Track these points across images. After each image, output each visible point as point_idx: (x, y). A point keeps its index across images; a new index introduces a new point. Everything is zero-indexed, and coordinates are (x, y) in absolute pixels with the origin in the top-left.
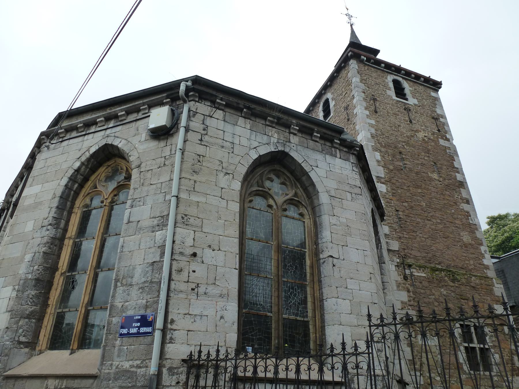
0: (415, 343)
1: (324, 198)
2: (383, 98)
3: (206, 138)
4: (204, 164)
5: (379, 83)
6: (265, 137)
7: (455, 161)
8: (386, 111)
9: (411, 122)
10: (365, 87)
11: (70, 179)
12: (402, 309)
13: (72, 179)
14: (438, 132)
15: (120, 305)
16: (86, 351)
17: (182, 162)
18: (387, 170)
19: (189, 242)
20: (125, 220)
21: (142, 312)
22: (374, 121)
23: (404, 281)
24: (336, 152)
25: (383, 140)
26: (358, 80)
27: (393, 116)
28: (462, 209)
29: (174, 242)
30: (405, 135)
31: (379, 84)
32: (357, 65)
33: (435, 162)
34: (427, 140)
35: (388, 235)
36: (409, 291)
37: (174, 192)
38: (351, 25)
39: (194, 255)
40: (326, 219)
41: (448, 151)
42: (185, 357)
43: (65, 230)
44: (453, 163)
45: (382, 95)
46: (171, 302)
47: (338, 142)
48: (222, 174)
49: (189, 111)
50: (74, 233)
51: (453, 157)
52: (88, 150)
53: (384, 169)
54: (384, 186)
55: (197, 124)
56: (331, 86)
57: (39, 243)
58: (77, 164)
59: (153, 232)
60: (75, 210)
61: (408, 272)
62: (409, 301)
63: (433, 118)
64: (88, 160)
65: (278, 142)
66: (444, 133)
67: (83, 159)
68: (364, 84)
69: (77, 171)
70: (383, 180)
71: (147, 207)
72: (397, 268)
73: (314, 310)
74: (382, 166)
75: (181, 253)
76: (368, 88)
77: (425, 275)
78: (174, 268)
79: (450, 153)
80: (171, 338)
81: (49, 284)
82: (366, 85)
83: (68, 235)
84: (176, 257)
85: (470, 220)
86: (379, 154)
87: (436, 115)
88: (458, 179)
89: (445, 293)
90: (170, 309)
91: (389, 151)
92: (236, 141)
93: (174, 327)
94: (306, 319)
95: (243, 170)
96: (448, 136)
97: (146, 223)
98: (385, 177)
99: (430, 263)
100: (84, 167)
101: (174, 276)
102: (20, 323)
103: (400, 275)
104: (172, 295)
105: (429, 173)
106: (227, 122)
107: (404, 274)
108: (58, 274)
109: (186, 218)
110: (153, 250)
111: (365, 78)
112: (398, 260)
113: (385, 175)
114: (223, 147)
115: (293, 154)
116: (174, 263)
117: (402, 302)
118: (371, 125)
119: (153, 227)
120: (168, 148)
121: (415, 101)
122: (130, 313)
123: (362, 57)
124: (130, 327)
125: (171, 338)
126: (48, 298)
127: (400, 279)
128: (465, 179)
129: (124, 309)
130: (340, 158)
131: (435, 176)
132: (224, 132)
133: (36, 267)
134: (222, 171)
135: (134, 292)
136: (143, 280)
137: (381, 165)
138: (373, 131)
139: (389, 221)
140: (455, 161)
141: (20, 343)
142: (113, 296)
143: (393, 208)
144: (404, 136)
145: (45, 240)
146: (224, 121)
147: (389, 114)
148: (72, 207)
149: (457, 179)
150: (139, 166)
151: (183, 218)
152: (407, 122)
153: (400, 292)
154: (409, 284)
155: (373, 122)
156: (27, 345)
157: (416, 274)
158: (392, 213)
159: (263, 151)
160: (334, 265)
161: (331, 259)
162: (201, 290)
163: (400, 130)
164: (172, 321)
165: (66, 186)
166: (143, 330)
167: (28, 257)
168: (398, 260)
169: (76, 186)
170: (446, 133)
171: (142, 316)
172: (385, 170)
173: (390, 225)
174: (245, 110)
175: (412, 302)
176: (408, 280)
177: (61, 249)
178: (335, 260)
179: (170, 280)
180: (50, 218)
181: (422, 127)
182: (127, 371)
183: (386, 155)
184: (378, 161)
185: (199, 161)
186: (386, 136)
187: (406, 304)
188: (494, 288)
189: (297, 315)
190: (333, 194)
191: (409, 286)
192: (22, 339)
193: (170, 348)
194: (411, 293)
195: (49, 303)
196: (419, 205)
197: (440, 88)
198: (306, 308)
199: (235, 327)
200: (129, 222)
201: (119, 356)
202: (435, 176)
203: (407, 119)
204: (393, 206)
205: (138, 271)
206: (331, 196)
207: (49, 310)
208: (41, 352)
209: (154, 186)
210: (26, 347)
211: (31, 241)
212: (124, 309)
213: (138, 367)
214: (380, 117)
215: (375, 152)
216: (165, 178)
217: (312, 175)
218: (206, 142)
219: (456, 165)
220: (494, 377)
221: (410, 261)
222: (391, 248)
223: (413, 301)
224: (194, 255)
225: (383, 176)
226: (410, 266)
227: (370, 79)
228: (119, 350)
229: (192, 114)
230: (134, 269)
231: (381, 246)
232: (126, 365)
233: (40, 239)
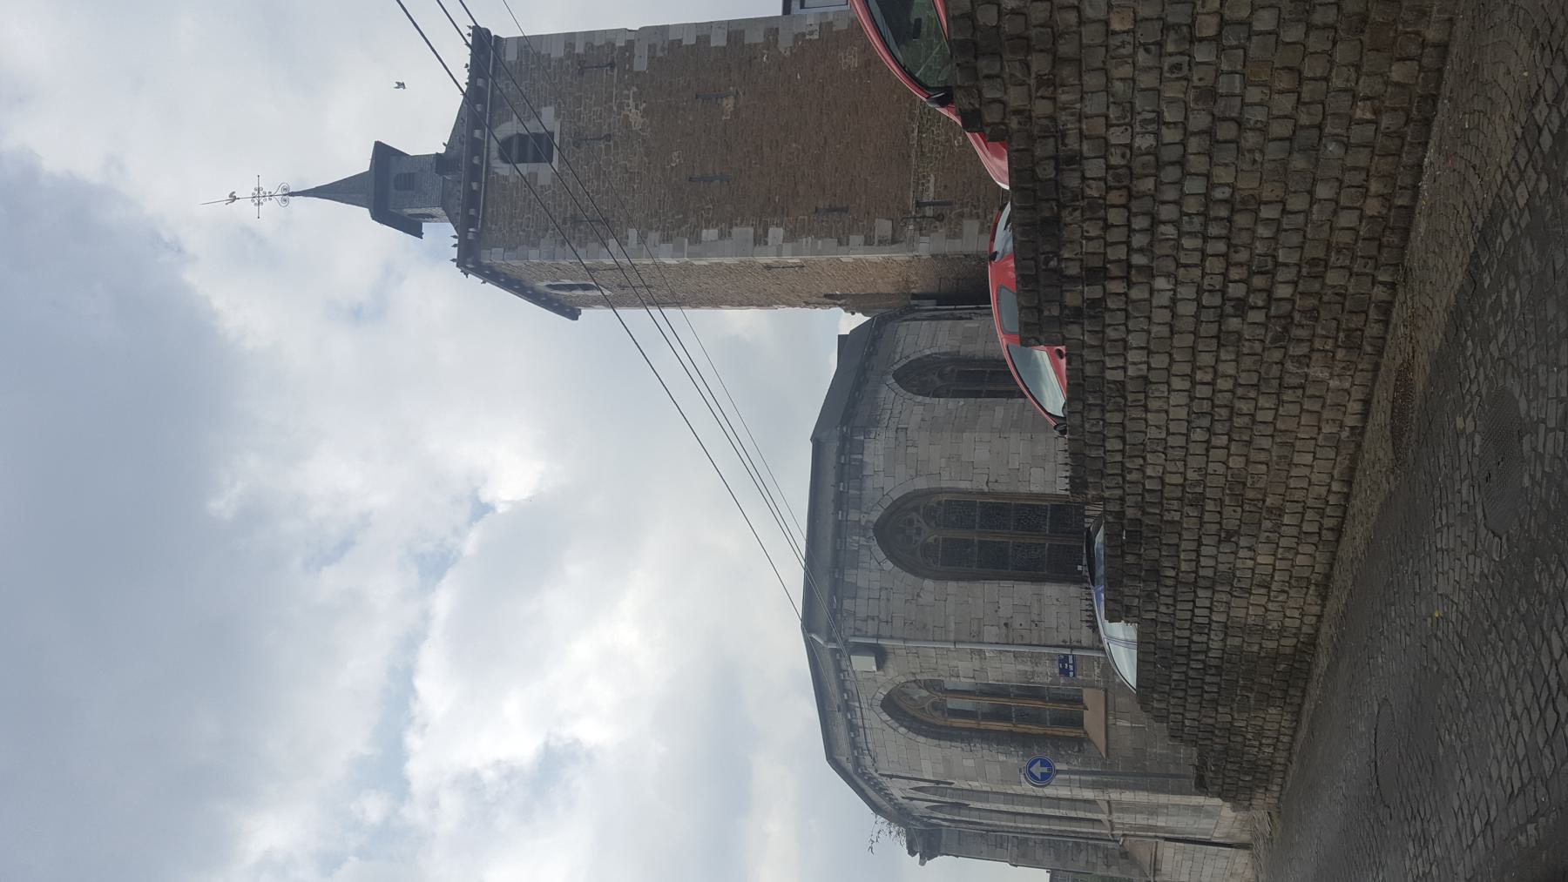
1: (922, 484)
2: (563, 198)
3: (882, 616)
4: (914, 618)
5: (525, 199)
6: (863, 551)
7: (681, 41)
8: (596, 197)
9: (608, 137)
10: (548, 236)
11: (918, 734)
13: (918, 732)
14: (616, 70)
15: (1051, 678)
16: (1085, 698)
17: (915, 640)
18: (737, 219)
19: (995, 630)
20: (973, 681)
21: (1056, 662)
22: (630, 230)
23: (945, 221)
24: (855, 460)
25: (670, 214)
26: (533, 253)
27: (604, 182)
28: (791, 51)
29: (997, 643)
30: (646, 159)
31: (527, 201)
32: (493, 249)
33: (694, 96)
34: (644, 105)
35: (865, 236)
36: (961, 215)
37: (952, 647)
38: (292, 194)
39: (1006, 625)
40: (945, 485)
41: (659, 54)
42: (1091, 631)
43: (970, 729)
44: (687, 46)
45: (558, 198)
46: (1049, 643)
47: (843, 457)
48: (920, 599)
49: (854, 636)
50: (973, 722)
51: (672, 42)
52: (885, 722)
53: (736, 225)
54: (772, 231)
55: (871, 627)
56: (519, 282)
57: (988, 751)
58: (902, 730)
59: (985, 659)
60: (948, 723)
61: (929, 211)
63: (581, 73)
64: (897, 720)
65: (864, 536)
66: (616, 53)
67: (897, 725)
68: (542, 240)
69: (909, 729)
70: (760, 231)
71: (960, 664)
72: (924, 232)
73: (1041, 500)
74: (731, 228)
75: (1007, 636)
76: (547, 230)
77: (932, 178)
78: (1020, 642)
79: (663, 49)
80: (1078, 642)
81: (1025, 735)
82: (540, 234)
83: (975, 726)
84: (1010, 642)
85: (811, 37)
86: (704, 231)
87: (569, 62)
88: (723, 43)
89: (960, 138)
90: (1055, 644)
91: (691, 206)
92: (877, 585)
93: (1068, 639)
94: (1049, 509)
95: (910, 578)
96: (620, 43)
97: (977, 664)
98: (752, 225)
99: (909, 156)
100: (905, 723)
101: (1028, 642)
102: (1063, 753)
103: (936, 227)
104: (1043, 643)
105: (724, 118)
106: (856, 594)
107: (934, 220)
108: (1014, 729)
109: (973, 634)
110: (1003, 658)
111: (521, 233)
112: (911, 227)
113: (748, 225)
114: (888, 600)
115: (875, 520)
116: (1015, 642)
118: (642, 238)
119: (981, 658)
120: (897, 651)
121: (548, 113)
122: (1057, 671)
123: (470, 237)
124: (1068, 670)
125: (1078, 642)
126: (1039, 734)
127: (943, 231)
128: (720, 24)
129: (1053, 675)
130: (862, 454)
131: (729, 104)
132: (869, 599)
133: (1013, 749)
134: (917, 600)
135: (1039, 669)
136: (1029, 663)
137: (727, 230)
138: (654, 236)
139: (841, 231)
140: (681, 41)
141: (1079, 751)
142: (1042, 684)
143: (812, 218)
144: (649, 163)
145: (985, 746)
146: (855, 598)
147: (602, 189)
148: (945, 727)
149: (725, 48)
150: (914, 674)
151: (974, 636)
152: (610, 146)
154: (950, 213)
155: (633, 233)
156: (1081, 745)
157: (932, 195)
158: (823, 221)
159: (881, 555)
160: (996, 481)
161: (989, 484)
162: (1036, 618)
163: (636, 170)
164: (1064, 641)
165: (926, 736)
166: (1071, 662)
167: (1002, 758)
168: (911, 227)
169: (924, 727)
170: (614, 45)
171: (1060, 663)
172: (739, 221)
173: (847, 231)
174: (837, 576)
175: (980, 211)
176: (944, 212)
177: (991, 731)
178: (990, 480)
179: (1031, 645)
180: (963, 745)
181: (615, 109)
182: (1102, 671)
183: (705, 216)
184: (722, 236)
185: (911, 623)
186: (660, 205)
187: (982, 224)
189: (1045, 517)
190: (913, 472)
191: (953, 213)
192: (1076, 749)
193: (1084, 644)
194: (965, 209)
195: (1042, 732)
196: (798, 158)
197: (488, 32)
198: (1038, 506)
199: (1064, 587)
200: (973, 678)
201: (1091, 676)
202: (729, 104)
203: (603, 147)
204: (809, 218)
205: (1021, 667)
206: (917, 474)
207: (1049, 732)
208: (1086, 733)
209: (939, 660)
210: (1082, 745)
211: (986, 758)
212: (1053, 675)
213: (1099, 663)
214: (616, 214)
215: (703, 239)
216: (933, 653)
217: (896, 495)
218: (887, 616)
219: (690, 40)
221: (911, 202)
222: (890, 237)
224: (1006, 625)
225: (751, 230)
226: (919, 204)
227: (520, 221)
228: (1087, 676)
229: (857, 632)
230: (1019, 671)
231: (936, 354)
232: (1097, 671)
233: (984, 751)
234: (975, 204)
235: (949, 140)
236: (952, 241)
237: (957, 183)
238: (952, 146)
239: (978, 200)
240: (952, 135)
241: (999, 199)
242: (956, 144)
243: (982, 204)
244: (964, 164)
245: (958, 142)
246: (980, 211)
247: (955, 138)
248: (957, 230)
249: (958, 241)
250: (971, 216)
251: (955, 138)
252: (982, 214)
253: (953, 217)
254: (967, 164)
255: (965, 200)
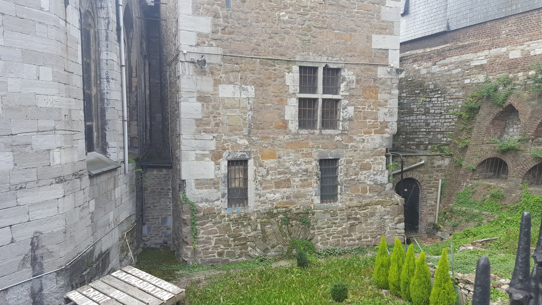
0: (211, 96)
12: (198, 45)
36: (216, 16)
62: (213, 32)
89: (287, 18)
117: (199, 35)
153: (198, 18)
154: (218, 5)
175: (220, 34)
187: (207, 36)
188: (383, 7)
191: (219, 8)
194: (221, 19)
220: (336, 137)
223: (222, 33)
234: (227, 29)
235: (285, 7)
236: (191, 5)
237: (247, 13)
238: (280, 9)
239: (230, 33)
240: (290, 9)
241: (231, 53)
242: (281, 14)
243: (226, 36)
244: (264, 21)
245: (283, 16)
246: (220, 34)
247: (287, 13)
248: (201, 11)
249: (190, 11)
250: (215, 25)
251: (287, 13)
252: (216, 36)
253: (215, 6)
254: (264, 23)
255: (230, 20)
